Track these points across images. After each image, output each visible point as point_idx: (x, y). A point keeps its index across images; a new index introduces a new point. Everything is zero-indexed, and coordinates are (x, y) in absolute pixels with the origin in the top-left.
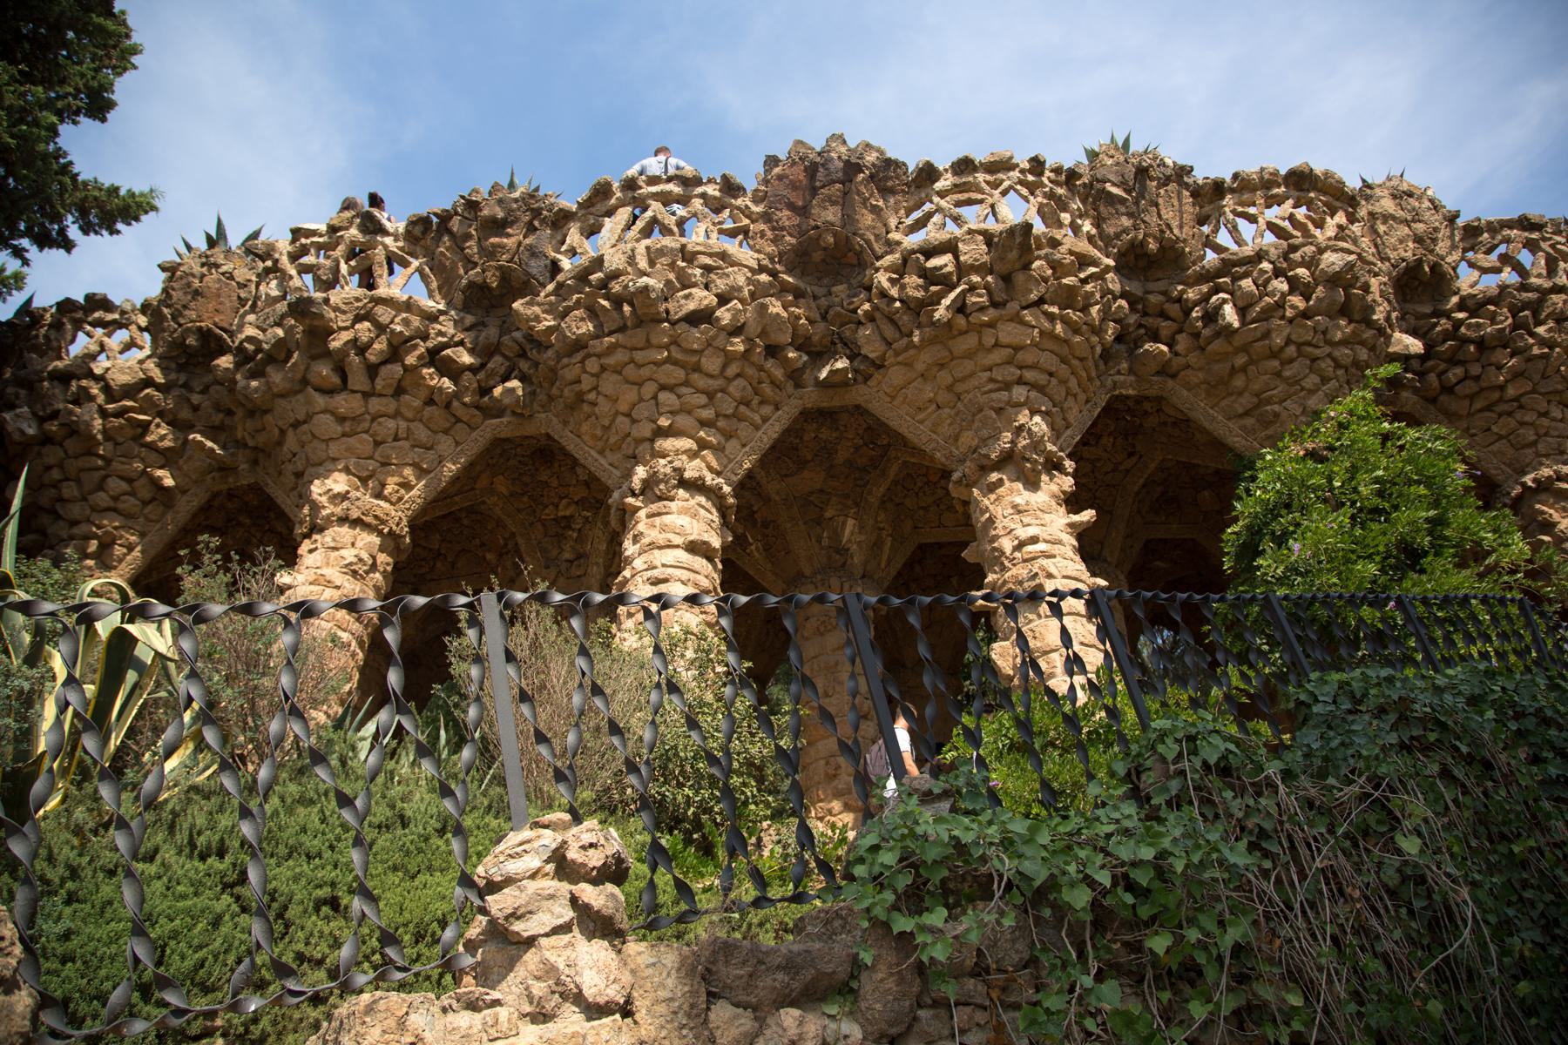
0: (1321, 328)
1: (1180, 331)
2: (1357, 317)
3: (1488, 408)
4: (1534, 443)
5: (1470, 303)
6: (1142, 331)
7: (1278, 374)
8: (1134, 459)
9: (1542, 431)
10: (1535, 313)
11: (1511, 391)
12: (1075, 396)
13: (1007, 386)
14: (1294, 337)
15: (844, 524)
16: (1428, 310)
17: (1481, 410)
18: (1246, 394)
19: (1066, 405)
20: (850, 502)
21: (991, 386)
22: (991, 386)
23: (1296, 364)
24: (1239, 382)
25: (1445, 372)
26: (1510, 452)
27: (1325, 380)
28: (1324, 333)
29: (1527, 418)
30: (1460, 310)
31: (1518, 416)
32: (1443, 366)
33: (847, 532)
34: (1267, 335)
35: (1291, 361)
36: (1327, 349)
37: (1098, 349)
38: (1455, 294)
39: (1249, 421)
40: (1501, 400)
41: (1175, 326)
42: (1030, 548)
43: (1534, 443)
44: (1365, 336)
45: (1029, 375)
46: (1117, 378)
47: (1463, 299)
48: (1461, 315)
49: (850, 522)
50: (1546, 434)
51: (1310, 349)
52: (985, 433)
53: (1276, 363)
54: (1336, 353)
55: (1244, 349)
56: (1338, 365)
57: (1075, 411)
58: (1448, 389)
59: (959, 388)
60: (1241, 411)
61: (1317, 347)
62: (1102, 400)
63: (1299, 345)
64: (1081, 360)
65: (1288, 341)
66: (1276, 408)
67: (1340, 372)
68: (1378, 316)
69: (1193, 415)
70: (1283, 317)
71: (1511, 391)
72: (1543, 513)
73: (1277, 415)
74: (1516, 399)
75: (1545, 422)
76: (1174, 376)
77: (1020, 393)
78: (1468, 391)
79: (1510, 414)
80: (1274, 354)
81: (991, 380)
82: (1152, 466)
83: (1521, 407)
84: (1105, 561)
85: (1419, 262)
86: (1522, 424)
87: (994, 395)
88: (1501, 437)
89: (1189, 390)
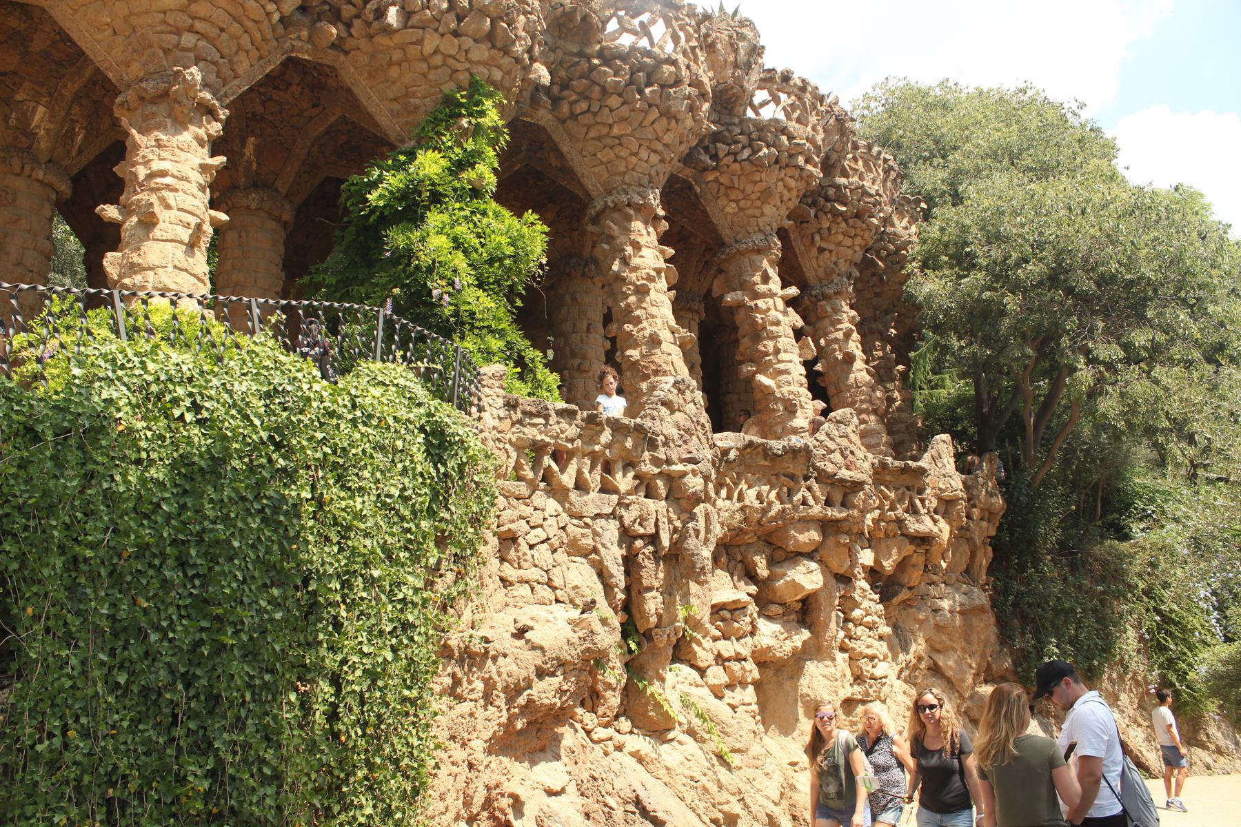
0: (465, 47)
1: (358, 16)
2: (499, 45)
3: (599, 139)
4: (624, 174)
5: (606, 53)
6: (327, 7)
7: (425, 75)
8: (317, 110)
9: (631, 167)
10: (649, 76)
11: (615, 131)
12: (247, 52)
13: (178, 32)
14: (442, 49)
15: (34, 110)
16: (575, 50)
17: (593, 139)
18: (398, 84)
19: (235, 59)
20: (44, 91)
21: (163, 27)
22: (163, 27)
23: (439, 71)
24: (394, 72)
25: (576, 102)
26: (606, 175)
28: (466, 52)
29: (622, 154)
30: (598, 58)
31: (617, 150)
32: (575, 97)
33: (37, 117)
34: (420, 42)
35: (437, 67)
36: (467, 66)
37: (276, 17)
38: (600, 42)
39: (396, 107)
40: (608, 135)
41: (353, 11)
42: (159, 180)
43: (624, 174)
44: (502, 61)
45: (199, 26)
46: (295, 43)
47: (602, 49)
48: (596, 61)
49: (41, 110)
50: (633, 169)
51: (451, 61)
52: (151, 68)
53: (425, 66)
54: (474, 70)
55: (402, 48)
57: (246, 64)
58: (574, 117)
59: (135, 21)
60: (391, 96)
61: (458, 61)
62: (279, 59)
63: (446, 56)
64: (256, 22)
65: (436, 52)
66: (417, 102)
68: (519, 48)
69: (356, 90)
70: (436, 30)
71: (615, 131)
72: (610, 228)
73: (417, 108)
74: (619, 137)
75: (634, 160)
76: (347, 53)
77: (188, 40)
78: (586, 121)
79: (611, 148)
80: (424, 59)
81: (165, 22)
82: (333, 119)
83: (620, 144)
84: (276, 190)
85: (574, 10)
86: (618, 157)
87: (164, 36)
88: (602, 163)
89: (356, 68)
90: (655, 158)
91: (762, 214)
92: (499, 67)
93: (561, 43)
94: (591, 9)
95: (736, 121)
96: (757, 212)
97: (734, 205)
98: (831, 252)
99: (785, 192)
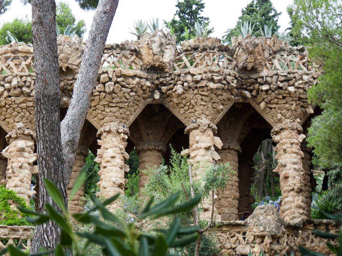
0: (13, 100)
16: (70, 78)
27: (19, 113)
28: (14, 101)
50: (106, 116)
54: (20, 106)
56: (22, 109)
63: (10, 105)
65: (6, 104)
67: (23, 110)
74: (95, 106)
90: (113, 109)
91: (196, 111)
92: (30, 101)
93: (65, 77)
94: (68, 64)
95: (168, 75)
96: (193, 110)
97: (182, 109)
98: (275, 108)
99: (203, 98)
